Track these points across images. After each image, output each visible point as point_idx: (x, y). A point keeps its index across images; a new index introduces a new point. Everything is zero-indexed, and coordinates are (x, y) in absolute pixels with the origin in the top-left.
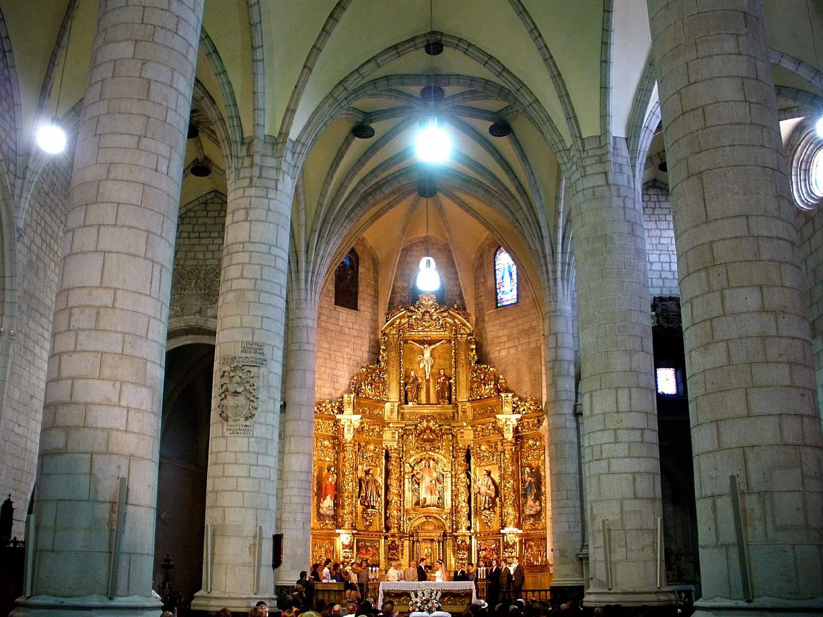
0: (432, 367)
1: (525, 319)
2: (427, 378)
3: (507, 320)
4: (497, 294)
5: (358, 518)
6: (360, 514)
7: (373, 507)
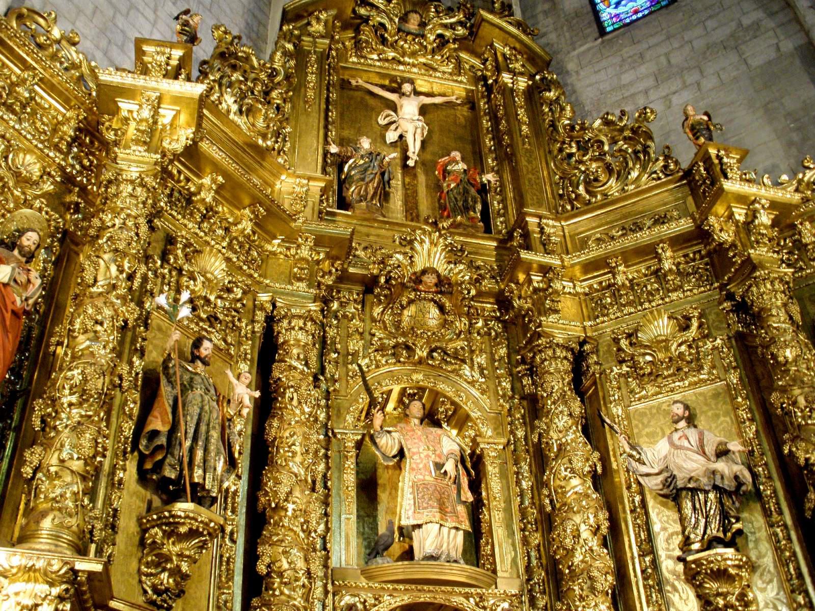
0: (423, 143)
1: (710, 24)
2: (411, 163)
3: (645, 46)
4: (596, 14)
5: (120, 538)
6: (128, 525)
7: (200, 496)
